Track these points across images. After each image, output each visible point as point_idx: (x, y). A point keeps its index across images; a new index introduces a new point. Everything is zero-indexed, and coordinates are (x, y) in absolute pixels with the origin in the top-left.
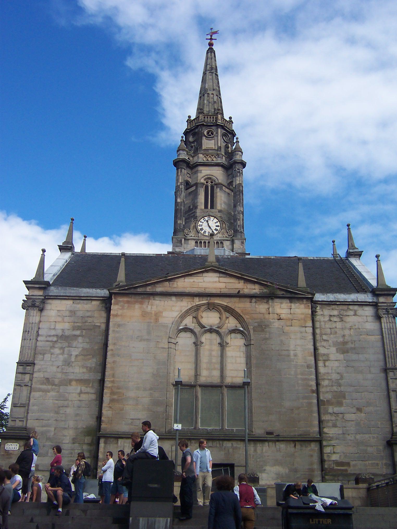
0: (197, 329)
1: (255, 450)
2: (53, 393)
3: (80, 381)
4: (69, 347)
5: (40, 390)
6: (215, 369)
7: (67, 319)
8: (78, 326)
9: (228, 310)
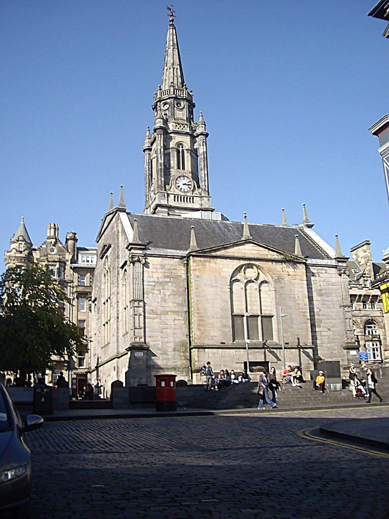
4: (163, 289)
5: (149, 318)
8: (168, 276)
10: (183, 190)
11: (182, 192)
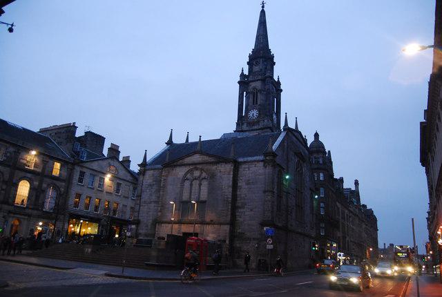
9: (202, 170)
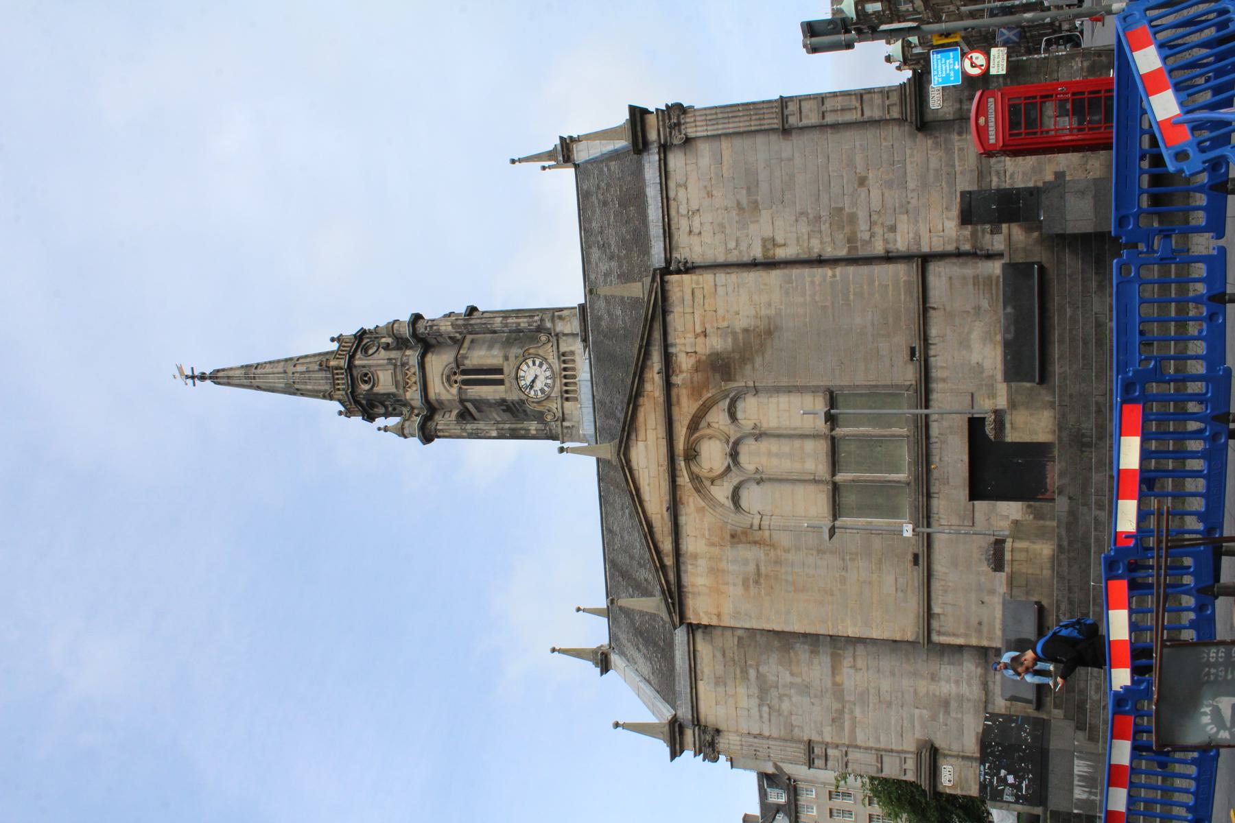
0: (734, 479)
1: (944, 380)
2: (858, 712)
3: (835, 669)
4: (777, 687)
5: (853, 731)
6: (802, 448)
7: (731, 690)
9: (694, 426)
10: (549, 381)
11: (554, 382)
